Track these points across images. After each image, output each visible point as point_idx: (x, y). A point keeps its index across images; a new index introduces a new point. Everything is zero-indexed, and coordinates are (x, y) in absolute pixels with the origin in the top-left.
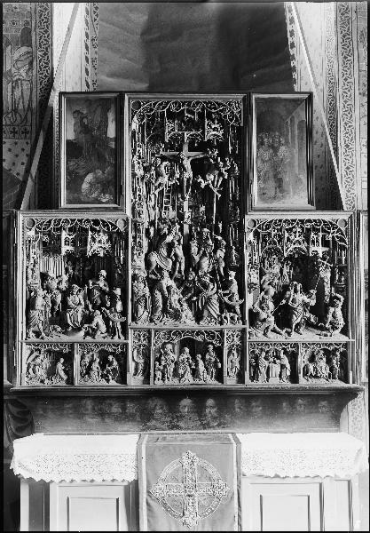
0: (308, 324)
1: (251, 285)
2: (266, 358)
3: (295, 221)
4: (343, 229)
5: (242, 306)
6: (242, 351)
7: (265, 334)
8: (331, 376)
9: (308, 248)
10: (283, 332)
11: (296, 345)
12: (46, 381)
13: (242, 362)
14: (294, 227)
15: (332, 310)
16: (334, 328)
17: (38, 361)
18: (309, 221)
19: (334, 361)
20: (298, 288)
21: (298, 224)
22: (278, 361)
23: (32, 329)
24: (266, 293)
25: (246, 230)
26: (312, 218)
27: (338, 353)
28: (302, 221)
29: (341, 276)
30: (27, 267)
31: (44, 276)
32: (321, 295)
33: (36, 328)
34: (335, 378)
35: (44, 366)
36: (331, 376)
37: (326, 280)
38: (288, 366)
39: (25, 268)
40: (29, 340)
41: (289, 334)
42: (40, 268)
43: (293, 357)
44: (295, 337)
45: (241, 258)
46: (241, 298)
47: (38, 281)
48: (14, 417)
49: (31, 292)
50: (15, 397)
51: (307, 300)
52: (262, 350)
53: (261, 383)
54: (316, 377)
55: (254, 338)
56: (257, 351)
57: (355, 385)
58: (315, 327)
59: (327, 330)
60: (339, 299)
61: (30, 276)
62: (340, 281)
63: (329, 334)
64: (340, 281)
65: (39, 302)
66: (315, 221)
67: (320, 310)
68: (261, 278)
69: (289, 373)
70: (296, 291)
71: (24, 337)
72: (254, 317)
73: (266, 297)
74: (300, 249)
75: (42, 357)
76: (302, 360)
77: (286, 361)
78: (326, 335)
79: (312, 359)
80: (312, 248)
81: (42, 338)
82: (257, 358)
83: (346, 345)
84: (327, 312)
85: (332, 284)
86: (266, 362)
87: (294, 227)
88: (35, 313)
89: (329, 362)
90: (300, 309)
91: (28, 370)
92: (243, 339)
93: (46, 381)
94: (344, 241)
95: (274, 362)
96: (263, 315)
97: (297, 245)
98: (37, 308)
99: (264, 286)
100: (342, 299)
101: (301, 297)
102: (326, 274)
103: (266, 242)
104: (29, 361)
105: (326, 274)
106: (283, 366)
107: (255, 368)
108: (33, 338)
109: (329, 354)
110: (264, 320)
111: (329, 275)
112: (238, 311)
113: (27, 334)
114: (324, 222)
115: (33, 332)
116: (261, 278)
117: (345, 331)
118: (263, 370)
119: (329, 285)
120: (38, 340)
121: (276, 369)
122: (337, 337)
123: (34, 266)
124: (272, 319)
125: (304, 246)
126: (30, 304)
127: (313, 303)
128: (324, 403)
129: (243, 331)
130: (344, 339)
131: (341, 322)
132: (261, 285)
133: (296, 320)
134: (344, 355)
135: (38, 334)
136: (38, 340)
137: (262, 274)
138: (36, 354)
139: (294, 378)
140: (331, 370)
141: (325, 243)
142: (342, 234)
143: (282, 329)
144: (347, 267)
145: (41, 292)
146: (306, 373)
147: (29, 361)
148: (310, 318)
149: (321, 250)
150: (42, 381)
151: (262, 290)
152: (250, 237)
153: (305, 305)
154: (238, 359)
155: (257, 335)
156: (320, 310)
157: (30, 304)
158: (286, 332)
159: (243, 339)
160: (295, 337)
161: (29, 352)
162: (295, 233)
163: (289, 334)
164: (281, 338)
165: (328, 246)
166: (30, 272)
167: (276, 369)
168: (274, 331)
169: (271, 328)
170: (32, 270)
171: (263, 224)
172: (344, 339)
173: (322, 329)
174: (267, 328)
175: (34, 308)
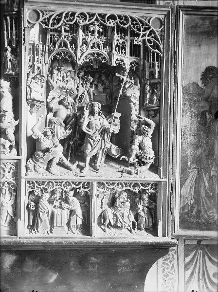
0: (109, 158)
1: (32, 103)
2: (51, 202)
3: (93, 15)
4: (157, 31)
5: (17, 130)
6: (16, 190)
7: (48, 169)
8: (136, 225)
9: (110, 54)
10: (74, 167)
11: (88, 184)
13: (16, 206)
14: (92, 24)
15: (138, 139)
16: (141, 163)
18: (112, 17)
19: (140, 207)
20: (97, 109)
21: (97, 20)
22: (65, 205)
24: (55, 114)
25: (26, 25)
26: (116, 13)
27: (145, 197)
28: (102, 16)
29: (153, 93)
32: (125, 121)
34: (140, 229)
36: (136, 225)
37: (132, 99)
38: (79, 212)
41: (81, 168)
43: (86, 201)
44: (88, 174)
45: (17, 65)
46: (16, 118)
51: (106, 123)
52: (43, 191)
53: (41, 235)
54: (116, 226)
55: (32, 175)
56: (38, 192)
57: (167, 239)
58: (117, 161)
59: (132, 165)
60: (148, 125)
62: (151, 101)
63: (134, 171)
64: (151, 101)
66: (120, 17)
67: (123, 140)
68: (47, 95)
69: (80, 222)
70: (92, 113)
72: (34, 145)
73: (54, 119)
74: (99, 55)
76: (98, 206)
77: (76, 204)
78: (130, 173)
79: (113, 203)
80: (116, 56)
82: (37, 201)
83: (156, 185)
84: (132, 142)
85: (142, 105)
86: (50, 208)
87: (92, 24)
89: (133, 207)
90: (97, 136)
92: (17, 175)
94: (158, 47)
95: (61, 208)
96: (46, 143)
97: (96, 50)
99: (51, 105)
100: (153, 124)
101: (99, 121)
102: (134, 93)
103: (54, 44)
105: (134, 93)
106: (72, 212)
107: (35, 214)
109: (134, 198)
110: (47, 150)
111: (137, 94)
112: (12, 136)
114: (133, 20)
116: (47, 95)
117: (154, 168)
118: (44, 217)
119: (137, 108)
121: (62, 216)
122: (145, 175)
124: (60, 148)
125: (104, 52)
127: (116, 129)
128: (124, 262)
129: (18, 164)
130: (153, 177)
131: (151, 154)
132: (47, 105)
133: (90, 152)
134: (153, 198)
137: (49, 88)
139: (86, 228)
140: (137, 217)
141: (135, 50)
142: (155, 37)
143: (73, 164)
144: (160, 84)
146: (102, 219)
148: (109, 150)
149: (128, 61)
151: (50, 110)
152: (32, 35)
153: (104, 131)
154: (11, 202)
155: (35, 172)
156: (123, 140)
158: (78, 166)
159: (17, 175)
160: (88, 174)
162: (93, 32)
163: (81, 168)
164: (72, 174)
165: (138, 55)
167: (62, 216)
168: (61, 164)
169: (56, 161)
171: (49, 19)
172: (153, 177)
173: (125, 163)
174: (50, 162)
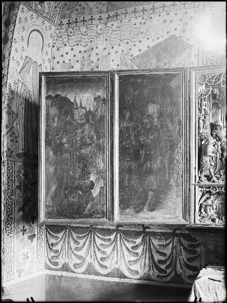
12: (217, 220)
17: (209, 202)
23: (204, 173)
30: (199, 118)
31: (213, 127)
33: (207, 173)
35: (215, 207)
39: (197, 119)
40: (202, 183)
42: (210, 120)
47: (208, 131)
48: (185, 248)
49: (202, 140)
50: (187, 232)
61: (201, 126)
65: (211, 149)
71: (197, 180)
75: (212, 198)
81: (214, 181)
88: (206, 159)
91: (200, 210)
93: (217, 220)
98: (209, 154)
104: (201, 202)
108: (205, 182)
113: (200, 177)
115: (205, 176)
120: (210, 183)
123: (205, 117)
126: (202, 151)
135: (209, 178)
136: (210, 183)
138: (207, 195)
145: (212, 140)
147: (201, 202)
150: (213, 220)
157: (202, 151)
161: (201, 194)
166: (201, 122)
170: (203, 120)
175: (206, 154)
